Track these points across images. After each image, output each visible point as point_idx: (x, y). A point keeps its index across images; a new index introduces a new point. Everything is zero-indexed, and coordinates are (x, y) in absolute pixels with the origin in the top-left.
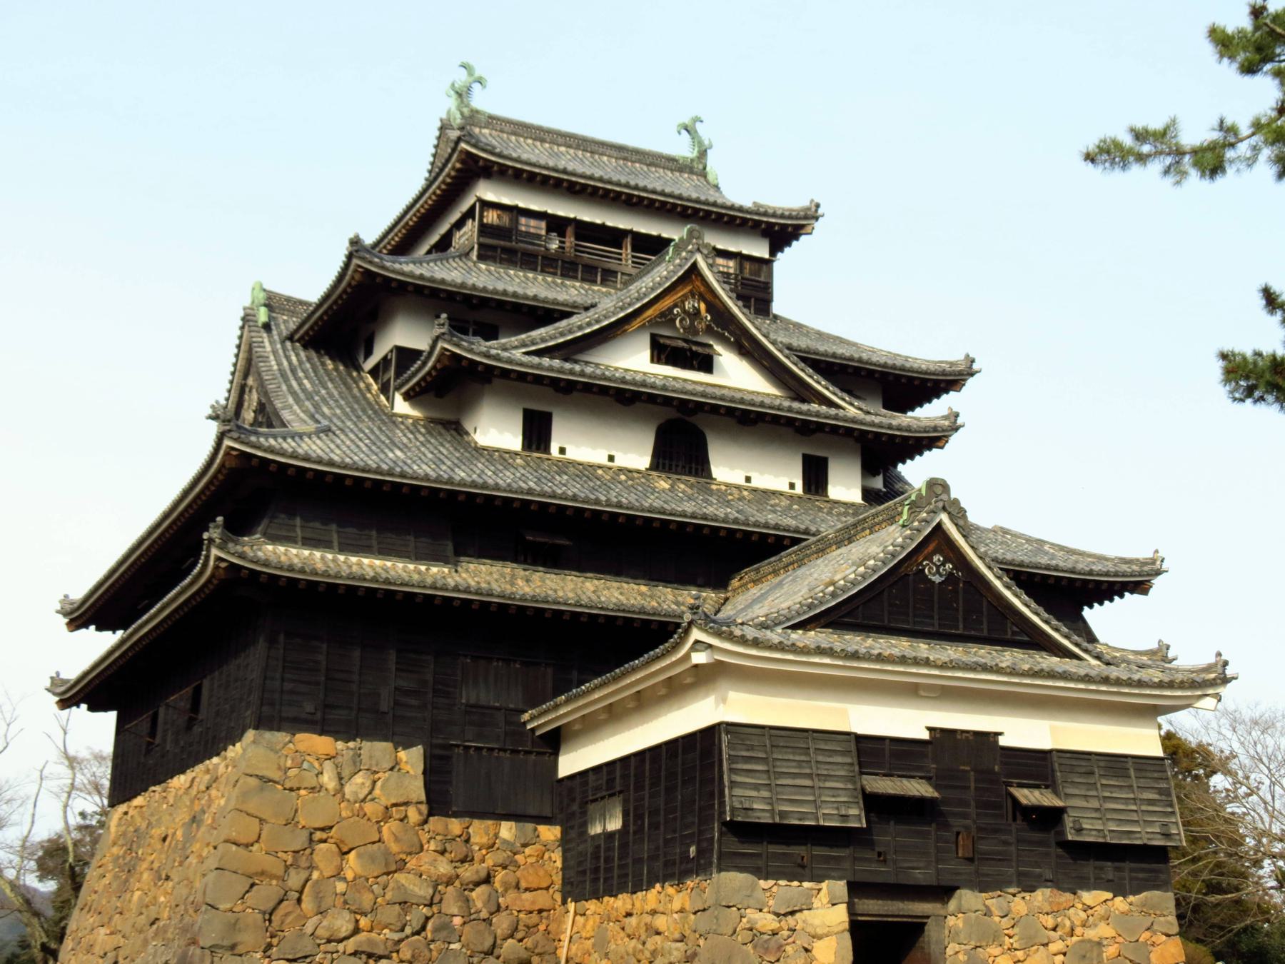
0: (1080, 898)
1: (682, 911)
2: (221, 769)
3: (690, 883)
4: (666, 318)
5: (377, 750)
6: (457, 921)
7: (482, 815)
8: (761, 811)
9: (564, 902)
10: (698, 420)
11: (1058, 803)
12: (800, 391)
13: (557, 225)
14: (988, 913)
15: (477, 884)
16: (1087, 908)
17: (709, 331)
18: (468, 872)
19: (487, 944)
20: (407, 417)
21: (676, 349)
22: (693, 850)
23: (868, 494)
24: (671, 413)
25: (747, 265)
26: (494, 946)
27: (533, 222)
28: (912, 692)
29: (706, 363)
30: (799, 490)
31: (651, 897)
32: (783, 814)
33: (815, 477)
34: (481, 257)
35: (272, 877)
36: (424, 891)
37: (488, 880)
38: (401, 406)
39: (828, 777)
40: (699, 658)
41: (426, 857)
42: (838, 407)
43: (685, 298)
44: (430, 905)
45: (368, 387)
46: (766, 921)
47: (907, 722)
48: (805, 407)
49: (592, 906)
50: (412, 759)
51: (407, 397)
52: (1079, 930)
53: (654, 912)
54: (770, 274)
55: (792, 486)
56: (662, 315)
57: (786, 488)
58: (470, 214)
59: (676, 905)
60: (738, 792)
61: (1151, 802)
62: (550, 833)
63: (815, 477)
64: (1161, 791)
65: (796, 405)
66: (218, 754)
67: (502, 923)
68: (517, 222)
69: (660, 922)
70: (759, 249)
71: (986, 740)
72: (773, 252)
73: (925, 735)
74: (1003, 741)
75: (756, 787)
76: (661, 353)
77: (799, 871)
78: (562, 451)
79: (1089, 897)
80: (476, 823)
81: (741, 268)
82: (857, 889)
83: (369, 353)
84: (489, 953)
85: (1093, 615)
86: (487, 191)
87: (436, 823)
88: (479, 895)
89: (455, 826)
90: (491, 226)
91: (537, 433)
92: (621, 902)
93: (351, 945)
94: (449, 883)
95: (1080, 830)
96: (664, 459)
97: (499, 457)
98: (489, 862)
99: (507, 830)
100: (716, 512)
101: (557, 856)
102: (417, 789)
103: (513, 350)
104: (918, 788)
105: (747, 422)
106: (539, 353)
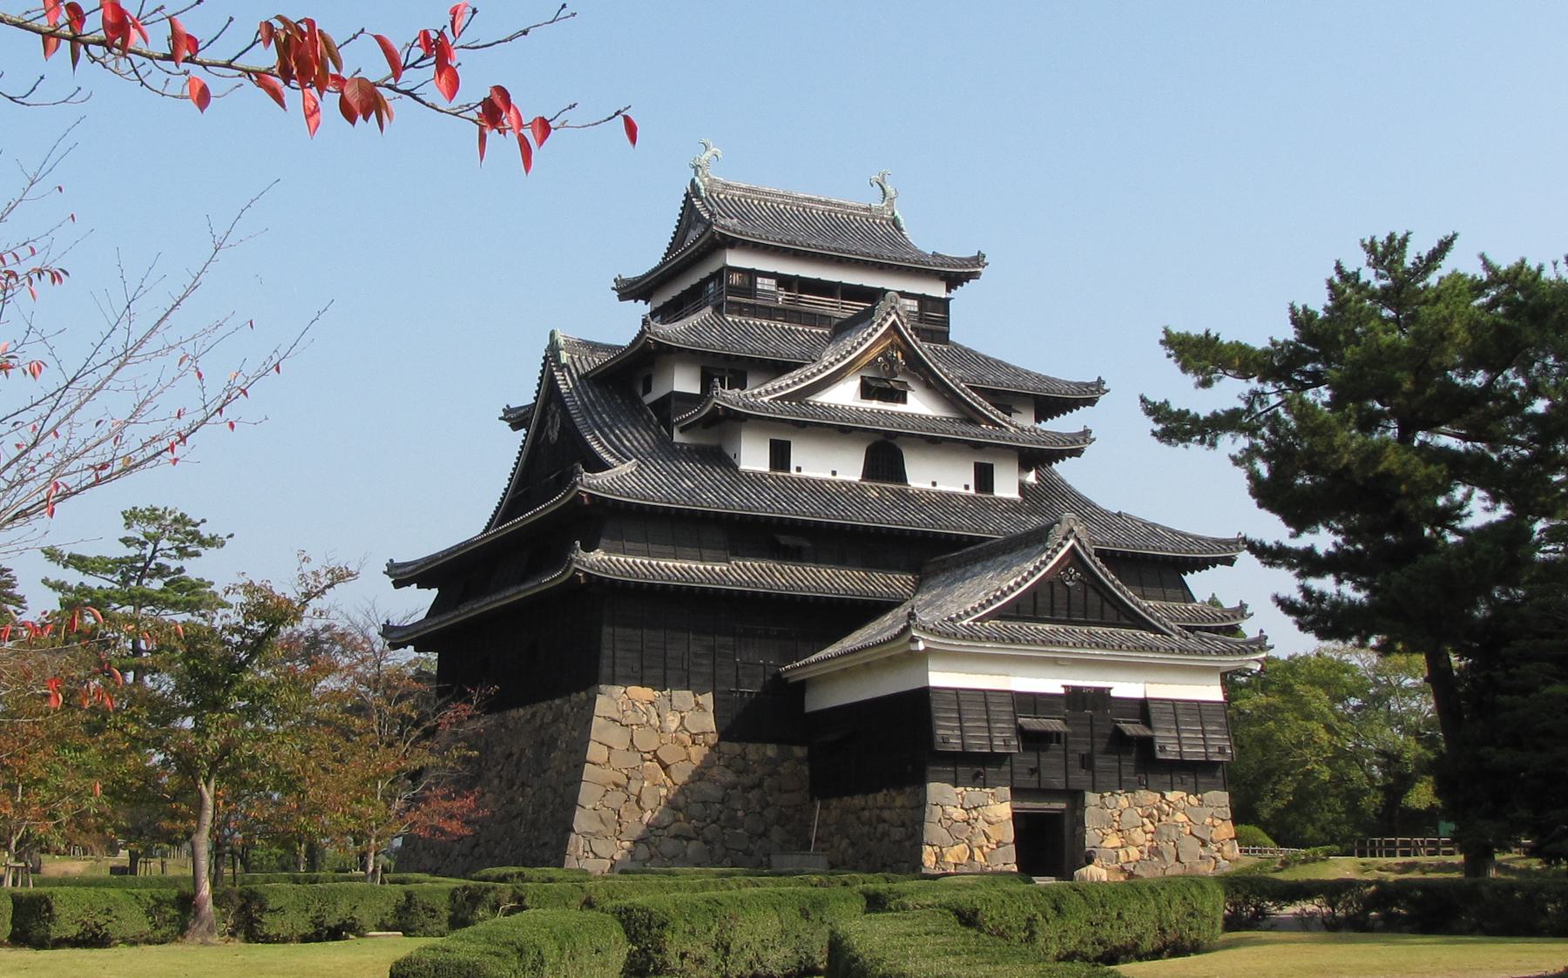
0: (1163, 796)
1: (903, 807)
2: (567, 708)
3: (908, 790)
4: (873, 364)
5: (684, 697)
6: (740, 813)
7: (754, 740)
8: (955, 744)
9: (812, 800)
10: (898, 443)
11: (1149, 733)
12: (971, 417)
13: (784, 281)
14: (1104, 806)
15: (753, 788)
16: (1169, 803)
17: (904, 372)
18: (746, 780)
19: (762, 828)
20: (682, 445)
21: (879, 389)
22: (909, 768)
23: (1023, 488)
24: (879, 437)
25: (929, 304)
26: (766, 830)
27: (766, 281)
28: (1055, 662)
29: (902, 399)
30: (972, 491)
31: (880, 797)
32: (971, 745)
33: (984, 479)
34: (729, 312)
35: (617, 785)
36: (719, 794)
37: (759, 785)
38: (678, 437)
39: (998, 721)
40: (913, 647)
41: (715, 771)
42: (1001, 426)
43: (886, 348)
44: (722, 802)
45: (650, 417)
46: (958, 814)
47: (1050, 683)
48: (977, 430)
49: (834, 802)
50: (707, 699)
51: (682, 430)
52: (1164, 818)
53: (882, 808)
54: (947, 312)
55: (967, 487)
56: (870, 363)
57: (962, 490)
58: (719, 276)
59: (899, 802)
60: (940, 732)
61: (1214, 732)
62: (800, 752)
63: (984, 479)
64: (1220, 725)
65: (972, 430)
66: (560, 696)
67: (770, 814)
68: (753, 283)
69: (886, 814)
70: (937, 290)
71: (1103, 694)
72: (948, 290)
73: (1062, 691)
74: (1114, 693)
75: (952, 729)
76: (867, 391)
77: (979, 781)
78: (799, 469)
79: (1170, 796)
80: (751, 747)
81: (920, 307)
82: (1017, 793)
83: (647, 390)
84: (764, 834)
85: (1191, 579)
86: (734, 259)
87: (725, 746)
88: (753, 795)
89: (737, 748)
90: (735, 287)
91: (780, 456)
92: (858, 801)
93: (673, 829)
94: (734, 787)
95: (1163, 749)
96: (872, 471)
97: (755, 479)
98: (760, 772)
99: (771, 751)
100: (916, 521)
101: (806, 769)
102: (709, 723)
103: (761, 394)
104: (1055, 725)
105: (932, 442)
106: (782, 398)
